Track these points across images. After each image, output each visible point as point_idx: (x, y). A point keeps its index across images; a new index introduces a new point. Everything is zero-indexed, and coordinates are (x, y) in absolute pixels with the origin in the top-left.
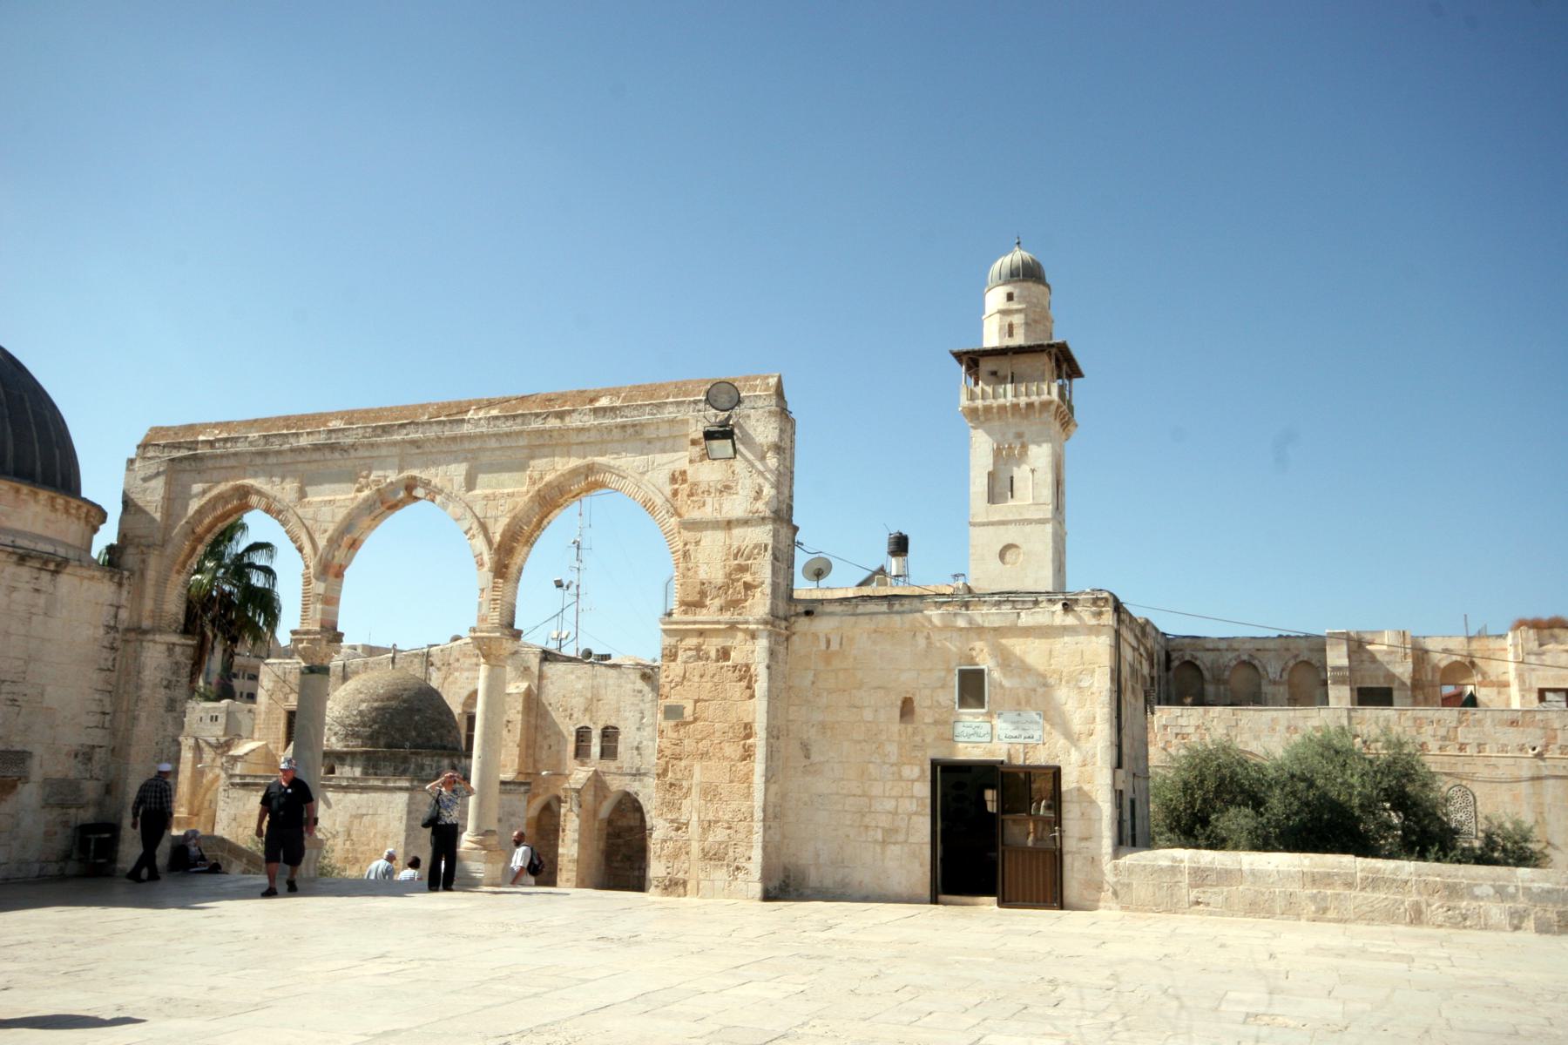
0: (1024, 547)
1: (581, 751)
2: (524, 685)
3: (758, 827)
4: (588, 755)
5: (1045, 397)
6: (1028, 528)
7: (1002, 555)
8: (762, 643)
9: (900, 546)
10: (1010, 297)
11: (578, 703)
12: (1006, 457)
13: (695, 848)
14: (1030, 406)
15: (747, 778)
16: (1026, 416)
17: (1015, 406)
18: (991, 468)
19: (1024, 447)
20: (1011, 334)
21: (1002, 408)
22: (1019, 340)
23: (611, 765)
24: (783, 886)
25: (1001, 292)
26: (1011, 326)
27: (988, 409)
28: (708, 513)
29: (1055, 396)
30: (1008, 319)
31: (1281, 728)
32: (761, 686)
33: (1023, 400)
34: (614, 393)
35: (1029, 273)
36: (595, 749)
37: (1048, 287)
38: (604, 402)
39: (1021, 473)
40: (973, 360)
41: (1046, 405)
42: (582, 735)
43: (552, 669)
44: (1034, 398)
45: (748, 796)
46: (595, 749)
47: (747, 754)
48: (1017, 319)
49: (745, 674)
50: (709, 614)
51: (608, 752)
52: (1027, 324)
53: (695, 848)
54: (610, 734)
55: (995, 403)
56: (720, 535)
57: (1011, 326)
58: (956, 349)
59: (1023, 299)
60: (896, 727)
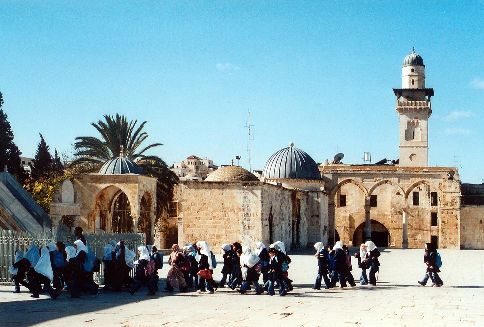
3: (459, 239)
7: (411, 157)
8: (459, 211)
10: (413, 70)
13: (448, 242)
14: (420, 109)
15: (457, 232)
16: (418, 112)
18: (407, 129)
20: (413, 83)
24: (462, 247)
26: (413, 80)
28: (447, 190)
30: (412, 78)
32: (459, 218)
33: (418, 107)
34: (426, 168)
37: (424, 66)
38: (424, 170)
39: (417, 130)
40: (399, 92)
44: (422, 107)
45: (457, 234)
47: (457, 228)
48: (416, 79)
49: (456, 216)
50: (449, 207)
52: (418, 80)
53: (448, 242)
56: (450, 194)
57: (413, 80)
58: (395, 88)
59: (417, 72)
60: (479, 224)
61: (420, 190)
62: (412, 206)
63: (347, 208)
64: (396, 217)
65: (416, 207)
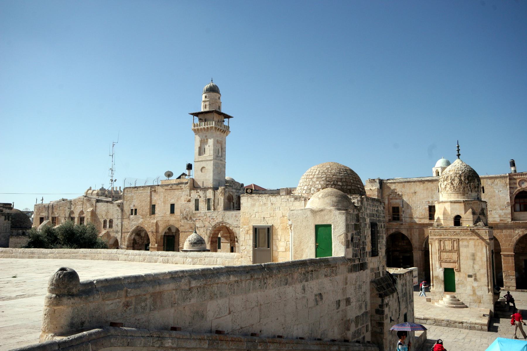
0: (207, 168)
1: (105, 226)
2: (92, 209)
4: (106, 227)
5: (211, 125)
6: (207, 162)
7: (201, 170)
9: (189, 167)
10: (206, 97)
11: (104, 213)
12: (203, 142)
14: (208, 128)
17: (204, 128)
19: (207, 139)
21: (201, 129)
22: (207, 109)
23: (111, 230)
25: (204, 96)
27: (198, 129)
29: (214, 125)
30: (205, 103)
31: (234, 216)
33: (206, 126)
35: (213, 90)
36: (108, 226)
39: (207, 147)
41: (212, 128)
42: (105, 222)
43: (99, 204)
44: (209, 126)
46: (108, 226)
48: (207, 103)
51: (111, 226)
52: (210, 104)
54: (111, 221)
55: (199, 127)
59: (209, 97)
61: (200, 197)
62: (194, 212)
63: (156, 215)
64: (183, 221)
65: (197, 212)
